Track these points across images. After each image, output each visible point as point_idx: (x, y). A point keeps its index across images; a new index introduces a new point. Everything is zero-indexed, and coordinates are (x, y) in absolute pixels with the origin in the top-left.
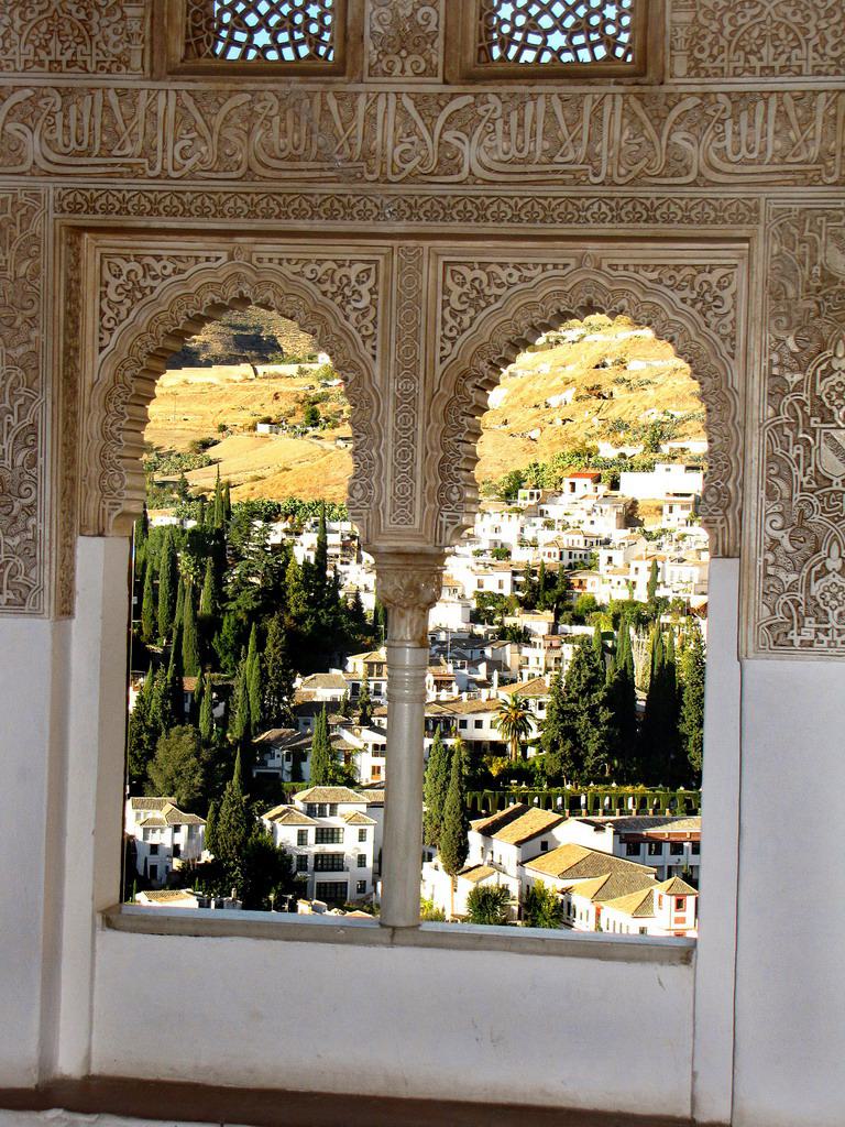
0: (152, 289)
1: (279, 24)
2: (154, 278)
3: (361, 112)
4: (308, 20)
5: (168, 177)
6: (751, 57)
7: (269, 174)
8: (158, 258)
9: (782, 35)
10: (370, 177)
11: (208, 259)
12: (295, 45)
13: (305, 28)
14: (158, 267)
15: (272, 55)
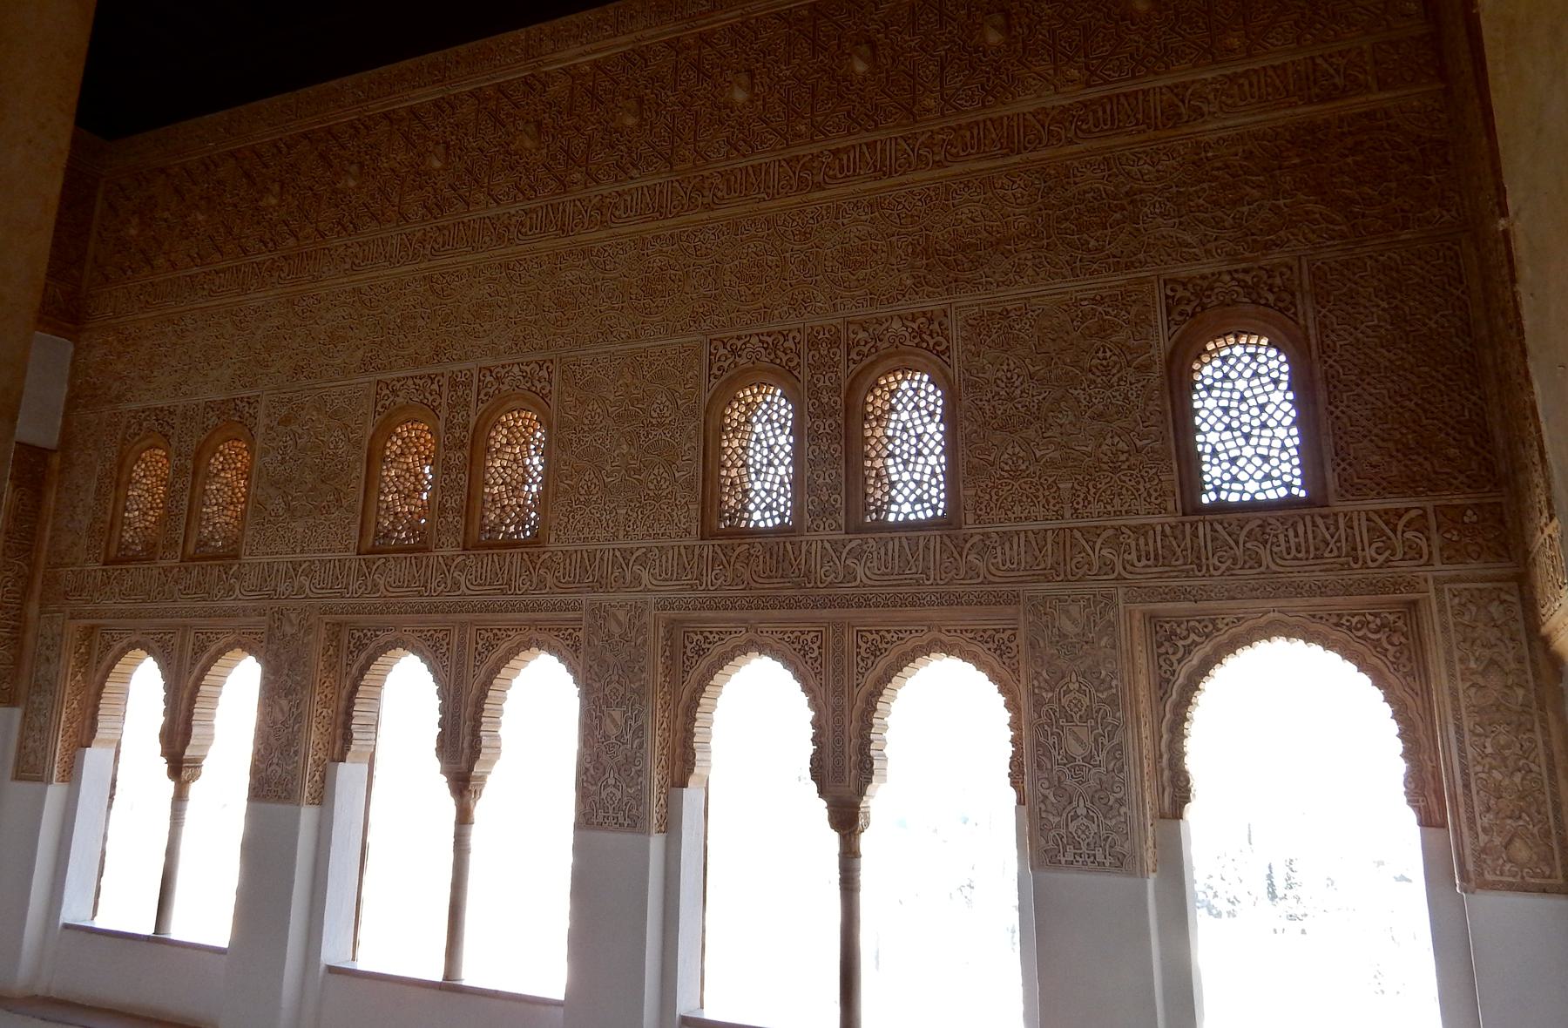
0: (886, 650)
1: (915, 500)
2: (887, 643)
3: (1049, 541)
4: (931, 497)
5: (937, 584)
6: (1108, 506)
7: (997, 580)
8: (888, 631)
9: (1124, 491)
10: (1059, 579)
11: (917, 631)
12: (924, 510)
13: (929, 501)
14: (888, 637)
15: (912, 517)
